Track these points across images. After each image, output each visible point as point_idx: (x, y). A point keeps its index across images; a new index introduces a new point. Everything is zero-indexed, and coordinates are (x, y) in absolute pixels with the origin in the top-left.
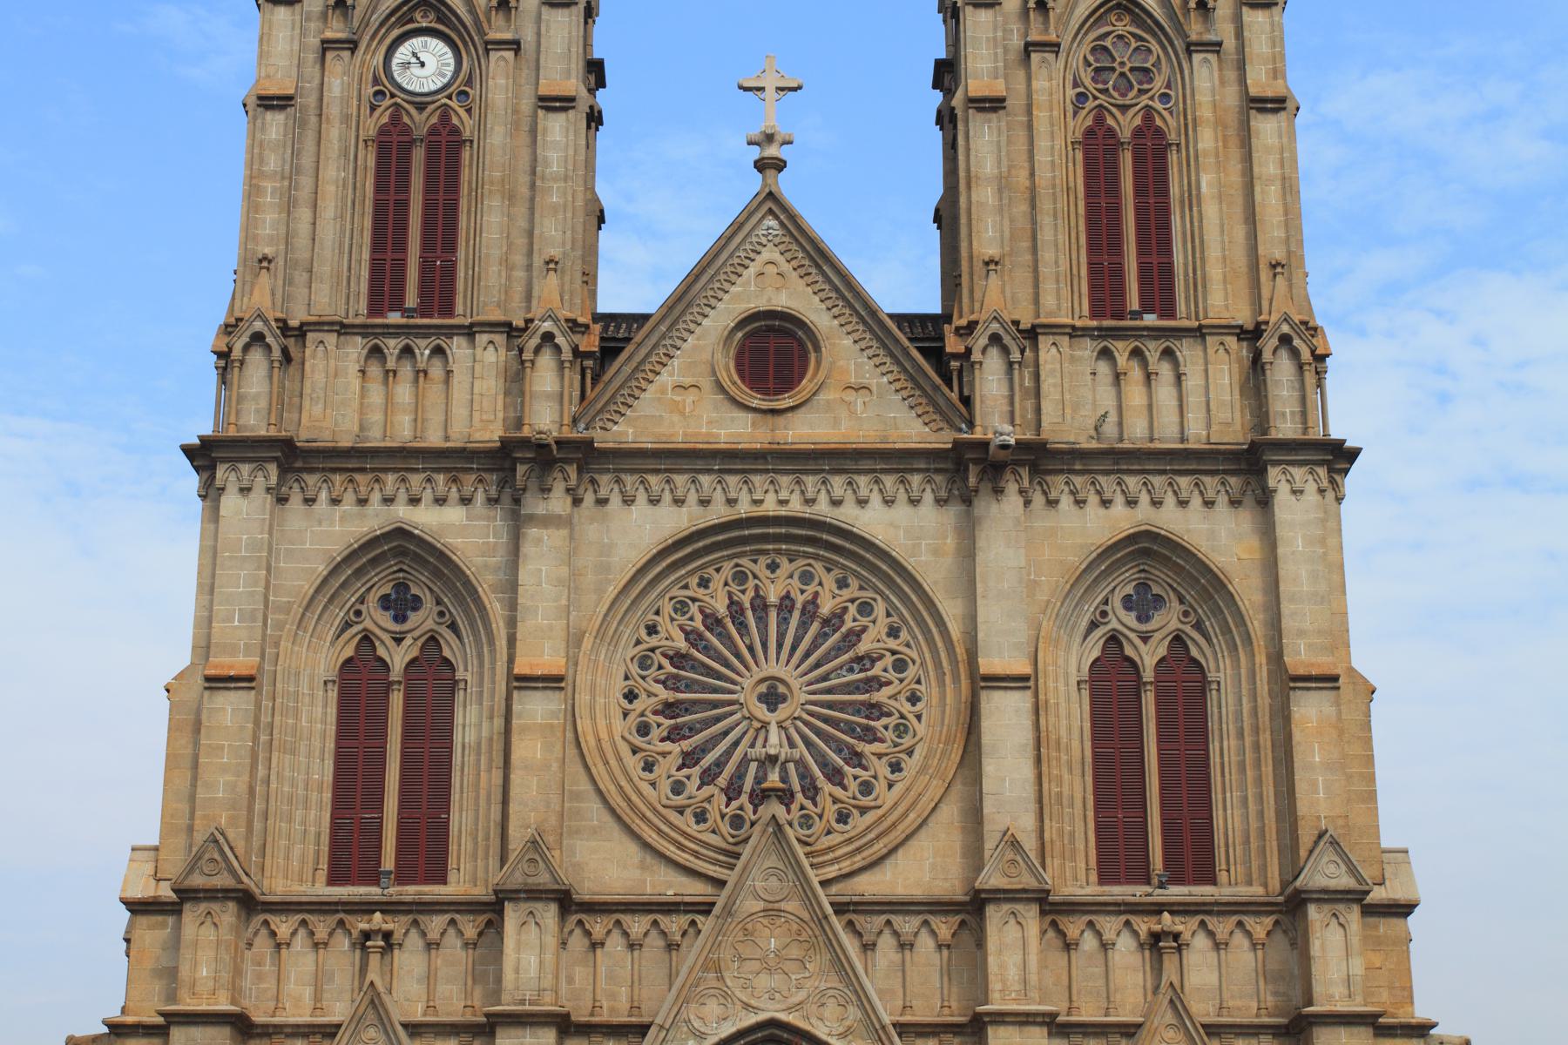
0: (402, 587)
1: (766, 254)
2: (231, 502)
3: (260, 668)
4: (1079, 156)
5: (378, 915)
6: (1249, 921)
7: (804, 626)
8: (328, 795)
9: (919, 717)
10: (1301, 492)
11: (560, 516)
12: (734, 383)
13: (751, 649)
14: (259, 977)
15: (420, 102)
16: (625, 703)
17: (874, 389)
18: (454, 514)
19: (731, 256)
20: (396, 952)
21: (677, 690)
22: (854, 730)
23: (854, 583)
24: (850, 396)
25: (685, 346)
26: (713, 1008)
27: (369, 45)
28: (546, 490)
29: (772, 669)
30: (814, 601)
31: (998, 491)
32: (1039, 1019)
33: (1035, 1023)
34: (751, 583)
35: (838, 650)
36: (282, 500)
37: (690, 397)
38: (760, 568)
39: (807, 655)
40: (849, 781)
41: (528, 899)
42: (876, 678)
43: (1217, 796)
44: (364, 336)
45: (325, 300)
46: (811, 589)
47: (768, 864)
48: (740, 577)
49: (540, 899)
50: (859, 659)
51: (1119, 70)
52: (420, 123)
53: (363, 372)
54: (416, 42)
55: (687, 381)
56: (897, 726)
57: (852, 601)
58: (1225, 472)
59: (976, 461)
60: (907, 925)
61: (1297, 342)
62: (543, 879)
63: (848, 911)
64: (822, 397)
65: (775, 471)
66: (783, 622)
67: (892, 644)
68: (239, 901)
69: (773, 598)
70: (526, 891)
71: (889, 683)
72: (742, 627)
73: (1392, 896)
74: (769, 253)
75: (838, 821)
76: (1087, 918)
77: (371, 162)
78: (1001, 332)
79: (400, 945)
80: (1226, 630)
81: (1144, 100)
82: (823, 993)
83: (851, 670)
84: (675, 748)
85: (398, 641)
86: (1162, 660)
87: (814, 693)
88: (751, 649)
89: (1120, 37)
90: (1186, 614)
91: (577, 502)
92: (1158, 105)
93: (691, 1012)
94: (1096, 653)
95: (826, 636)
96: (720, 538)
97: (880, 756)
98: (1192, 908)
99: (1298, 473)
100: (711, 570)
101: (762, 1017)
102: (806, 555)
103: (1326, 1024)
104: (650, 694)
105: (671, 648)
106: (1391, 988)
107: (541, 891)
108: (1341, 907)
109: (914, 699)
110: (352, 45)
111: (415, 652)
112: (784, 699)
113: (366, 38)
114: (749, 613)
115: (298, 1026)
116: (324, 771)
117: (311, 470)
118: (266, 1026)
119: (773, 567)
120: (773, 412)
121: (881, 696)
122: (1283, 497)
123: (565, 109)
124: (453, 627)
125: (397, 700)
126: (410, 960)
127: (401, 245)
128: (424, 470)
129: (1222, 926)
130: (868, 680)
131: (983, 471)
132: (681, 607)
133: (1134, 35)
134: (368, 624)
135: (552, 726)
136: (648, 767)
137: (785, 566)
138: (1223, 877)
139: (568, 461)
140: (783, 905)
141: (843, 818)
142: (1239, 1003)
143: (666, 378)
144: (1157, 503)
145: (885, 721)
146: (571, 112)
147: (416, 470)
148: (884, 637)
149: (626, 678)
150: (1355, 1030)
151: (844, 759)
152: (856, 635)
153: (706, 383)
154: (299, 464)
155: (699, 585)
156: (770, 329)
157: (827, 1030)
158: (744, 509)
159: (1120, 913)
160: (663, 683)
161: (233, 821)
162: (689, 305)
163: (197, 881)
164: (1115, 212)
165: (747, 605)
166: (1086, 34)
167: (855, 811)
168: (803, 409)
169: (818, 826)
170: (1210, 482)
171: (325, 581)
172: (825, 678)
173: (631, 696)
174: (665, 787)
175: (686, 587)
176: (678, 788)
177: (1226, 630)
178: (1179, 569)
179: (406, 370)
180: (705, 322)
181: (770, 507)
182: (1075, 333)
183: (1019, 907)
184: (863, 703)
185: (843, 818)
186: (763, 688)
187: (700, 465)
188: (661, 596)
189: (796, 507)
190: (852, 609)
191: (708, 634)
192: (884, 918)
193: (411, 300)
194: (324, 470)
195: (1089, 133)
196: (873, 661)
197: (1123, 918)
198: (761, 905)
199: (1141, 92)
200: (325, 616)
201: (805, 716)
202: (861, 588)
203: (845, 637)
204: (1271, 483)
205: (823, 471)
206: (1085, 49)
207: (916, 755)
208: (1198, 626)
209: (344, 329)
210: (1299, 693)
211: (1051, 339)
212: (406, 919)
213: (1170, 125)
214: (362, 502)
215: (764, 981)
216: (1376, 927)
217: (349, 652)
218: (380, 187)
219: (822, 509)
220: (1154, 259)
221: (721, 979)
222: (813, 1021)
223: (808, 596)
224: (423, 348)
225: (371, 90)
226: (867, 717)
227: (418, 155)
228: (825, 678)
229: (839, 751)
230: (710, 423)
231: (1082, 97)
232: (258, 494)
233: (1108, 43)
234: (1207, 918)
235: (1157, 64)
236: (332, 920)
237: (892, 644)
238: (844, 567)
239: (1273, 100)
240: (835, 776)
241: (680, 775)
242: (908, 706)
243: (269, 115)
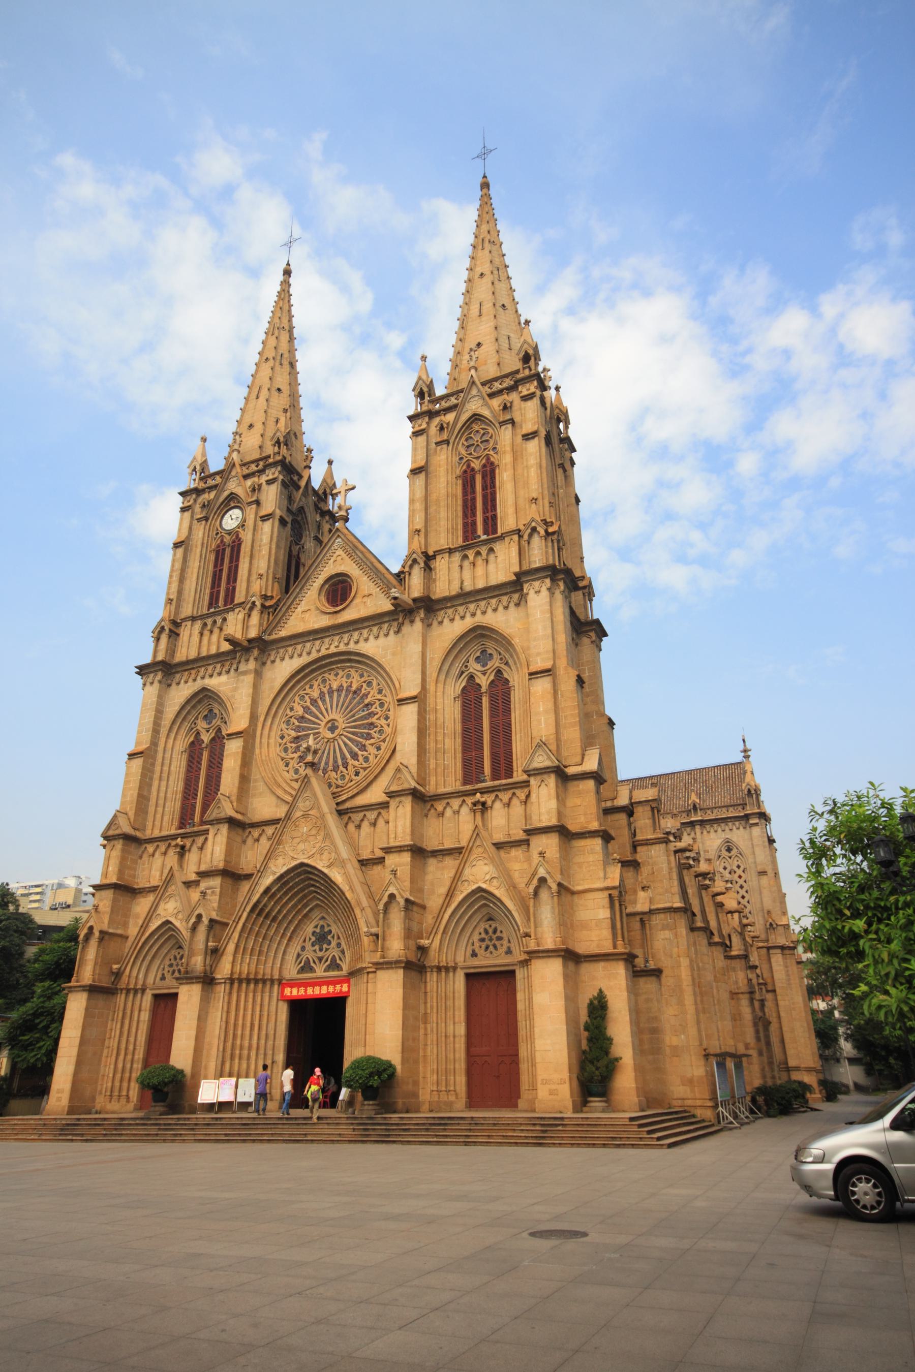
0: (211, 711)
1: (337, 553)
2: (148, 687)
3: (148, 749)
4: (460, 482)
5: (179, 839)
6: (518, 792)
7: (346, 696)
8: (179, 796)
9: (388, 725)
10: (539, 592)
11: (251, 670)
12: (324, 605)
13: (327, 710)
14: (143, 870)
15: (229, 533)
16: (280, 741)
17: (374, 594)
18: (224, 678)
19: (324, 557)
20: (187, 854)
21: (299, 732)
22: (363, 736)
23: (365, 674)
24: (365, 599)
25: (307, 595)
26: (280, 861)
27: (213, 517)
28: (247, 660)
29: (332, 717)
30: (351, 686)
31: (412, 622)
32: (406, 849)
33: (404, 851)
34: (328, 682)
35: (359, 703)
36: (169, 686)
37: (307, 615)
38: (332, 677)
39: (347, 707)
40: (361, 758)
41: (218, 823)
42: (372, 712)
43: (513, 738)
44: (201, 619)
45: (187, 610)
46: (349, 681)
47: (305, 795)
48: (324, 681)
49: (221, 823)
50: (367, 705)
51: (476, 444)
52: (227, 539)
53: (201, 634)
54: (230, 512)
55: (306, 608)
56: (380, 731)
57: (365, 682)
58: (511, 592)
59: (402, 611)
60: (372, 815)
61: (538, 529)
62: (222, 815)
63: (348, 813)
64: (355, 602)
65: (333, 635)
66: (339, 696)
67: (379, 697)
68: (123, 838)
69: (335, 687)
70: (217, 820)
71: (377, 713)
72: (324, 701)
73: (583, 769)
74: (340, 552)
75: (355, 775)
76: (446, 801)
77: (213, 557)
78: (417, 557)
79: (189, 850)
80: (515, 664)
81: (486, 452)
82: (322, 849)
83: (363, 711)
84: (296, 755)
85: (208, 731)
86: (493, 681)
87: (349, 723)
88: (327, 710)
89: (477, 431)
90: (501, 659)
91: (264, 664)
92: (491, 453)
93: (271, 864)
94: (464, 684)
95: (355, 698)
96: (314, 667)
97: (372, 745)
98: (491, 789)
99: (536, 584)
100: (314, 681)
101: (298, 862)
102: (348, 667)
103: (535, 834)
104: (289, 735)
105: (298, 715)
106: (585, 814)
107: (221, 819)
108: (545, 776)
109: (387, 718)
110: (206, 519)
111: (213, 735)
112: (337, 728)
113: (212, 515)
114: (327, 696)
115: (150, 887)
116: (181, 786)
117: (178, 672)
118: (140, 889)
119: (336, 675)
120: (336, 612)
121: (374, 720)
122: (532, 596)
123: (269, 519)
124: (226, 723)
125: (205, 755)
126: (192, 858)
127: (219, 586)
128: (213, 663)
129: (504, 797)
130: (369, 714)
131: (406, 615)
132: (302, 698)
133: (483, 429)
134: (199, 727)
135: (238, 752)
136: (287, 765)
137: (341, 673)
138: (515, 774)
139: (253, 648)
140: (310, 812)
141: (357, 774)
142: (514, 832)
143: (299, 609)
144: (484, 613)
145: (375, 729)
146: (271, 520)
147: (210, 664)
148: (376, 694)
149: (282, 730)
150: (549, 835)
151: (359, 749)
152: (366, 695)
153: (313, 608)
154: (174, 671)
155: (310, 688)
156: (339, 581)
157: (322, 865)
158: (324, 652)
159: (460, 796)
160: (294, 730)
161: (131, 808)
162: (308, 580)
163: (111, 833)
164: (474, 499)
165: (326, 692)
166: (463, 434)
167: (361, 771)
168: (347, 609)
169: (347, 777)
170: (505, 599)
171: (179, 712)
172: (354, 716)
173: (282, 737)
174: (292, 772)
175: (305, 690)
176: (297, 771)
177: (515, 664)
178: (496, 640)
179: (216, 631)
180: (315, 584)
181: (333, 650)
182: (451, 551)
183: (403, 798)
184: (367, 724)
185: (357, 774)
186: (330, 725)
187: (305, 639)
188: (295, 695)
189: (342, 648)
190: (365, 685)
191: (311, 707)
192: (361, 815)
193: (221, 603)
194: (182, 671)
195: (465, 472)
196: (372, 705)
197: (462, 799)
198: (302, 813)
199: (485, 449)
200: (184, 727)
201: (345, 733)
202: (369, 676)
203: (362, 698)
204: (525, 591)
205: (350, 631)
206: (463, 439)
207: (386, 742)
208: (507, 664)
209: (193, 619)
210: (533, 680)
211: (441, 556)
212: (191, 839)
213: (494, 458)
214: (195, 680)
215: (301, 846)
216: (578, 786)
217: (192, 739)
218: (215, 566)
219: (352, 647)
220: (489, 514)
221: (284, 847)
222: (318, 862)
223: (349, 684)
224: (219, 620)
225: (215, 533)
226: (369, 729)
227: (228, 551)
228: (354, 716)
229: (357, 746)
230: (313, 622)
231: (461, 459)
232: (156, 685)
233: (472, 435)
234: (498, 793)
235: (491, 437)
236: (167, 843)
237: (379, 697)
238: (362, 669)
239: (531, 434)
240: (355, 756)
241: (297, 767)
242: (385, 722)
243: (177, 550)
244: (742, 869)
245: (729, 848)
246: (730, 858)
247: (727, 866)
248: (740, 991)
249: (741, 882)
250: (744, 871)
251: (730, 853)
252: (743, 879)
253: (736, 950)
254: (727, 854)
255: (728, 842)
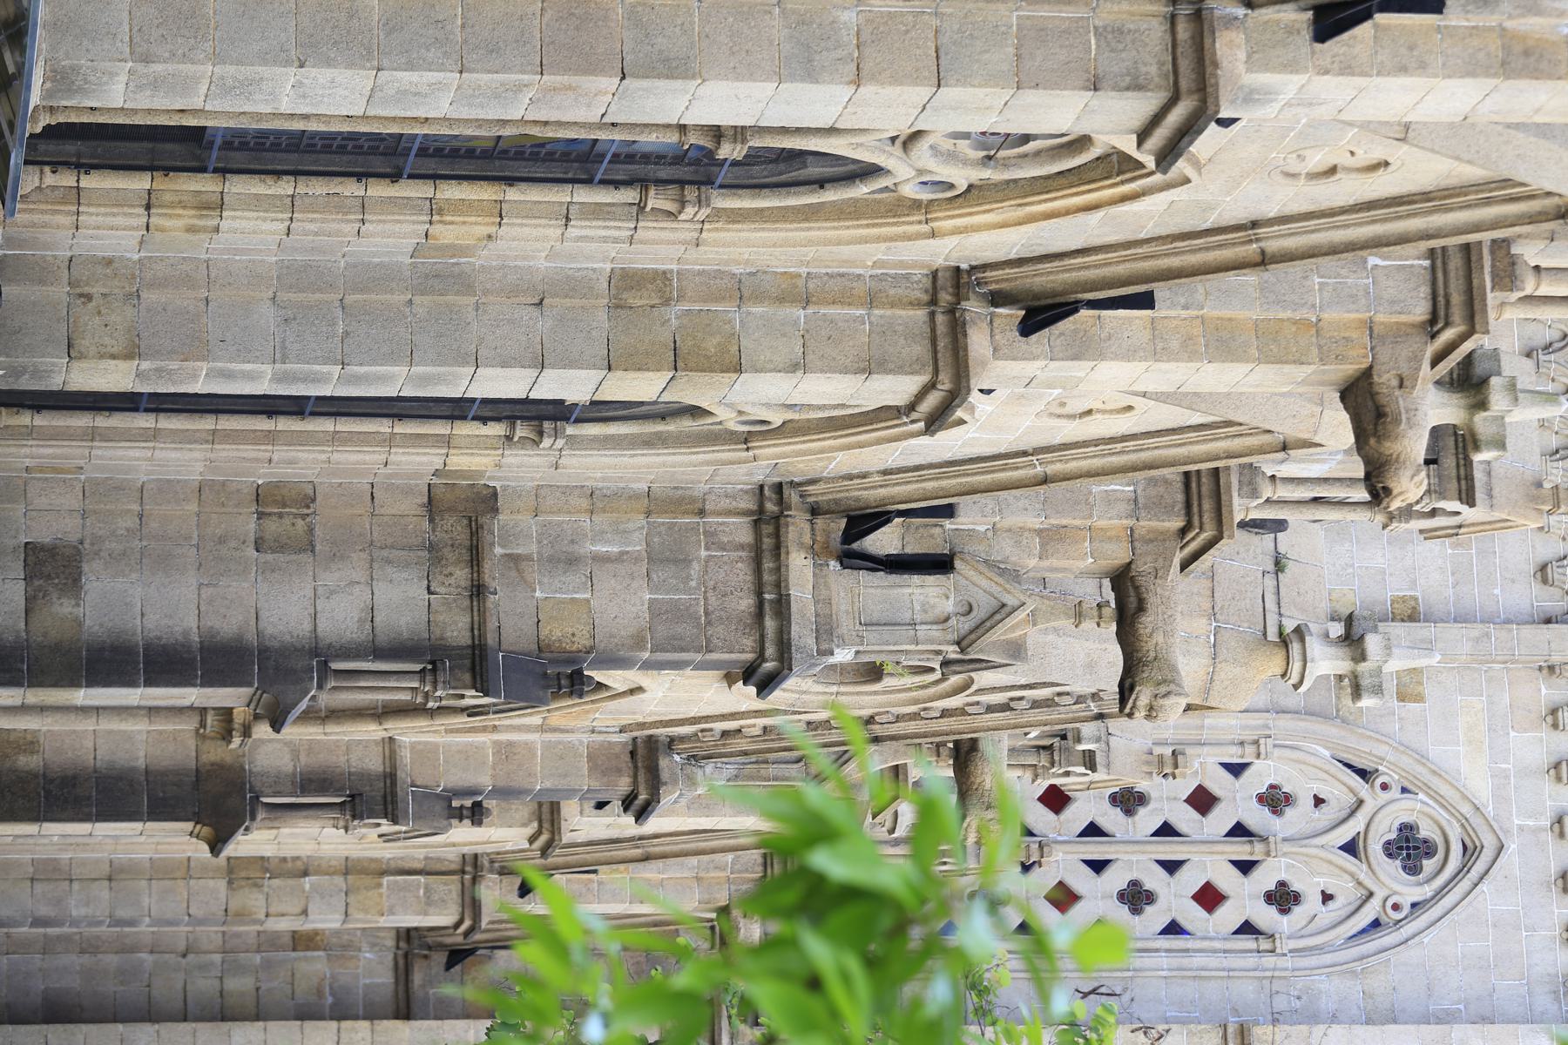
244: (1266, 916)
245: (1428, 849)
246: (1350, 848)
247: (1298, 818)
248: (492, 574)
249: (1174, 897)
250: (1247, 928)
251: (1390, 850)
252: (1192, 915)
253: (823, 601)
254: (1385, 830)
255: (1470, 851)
